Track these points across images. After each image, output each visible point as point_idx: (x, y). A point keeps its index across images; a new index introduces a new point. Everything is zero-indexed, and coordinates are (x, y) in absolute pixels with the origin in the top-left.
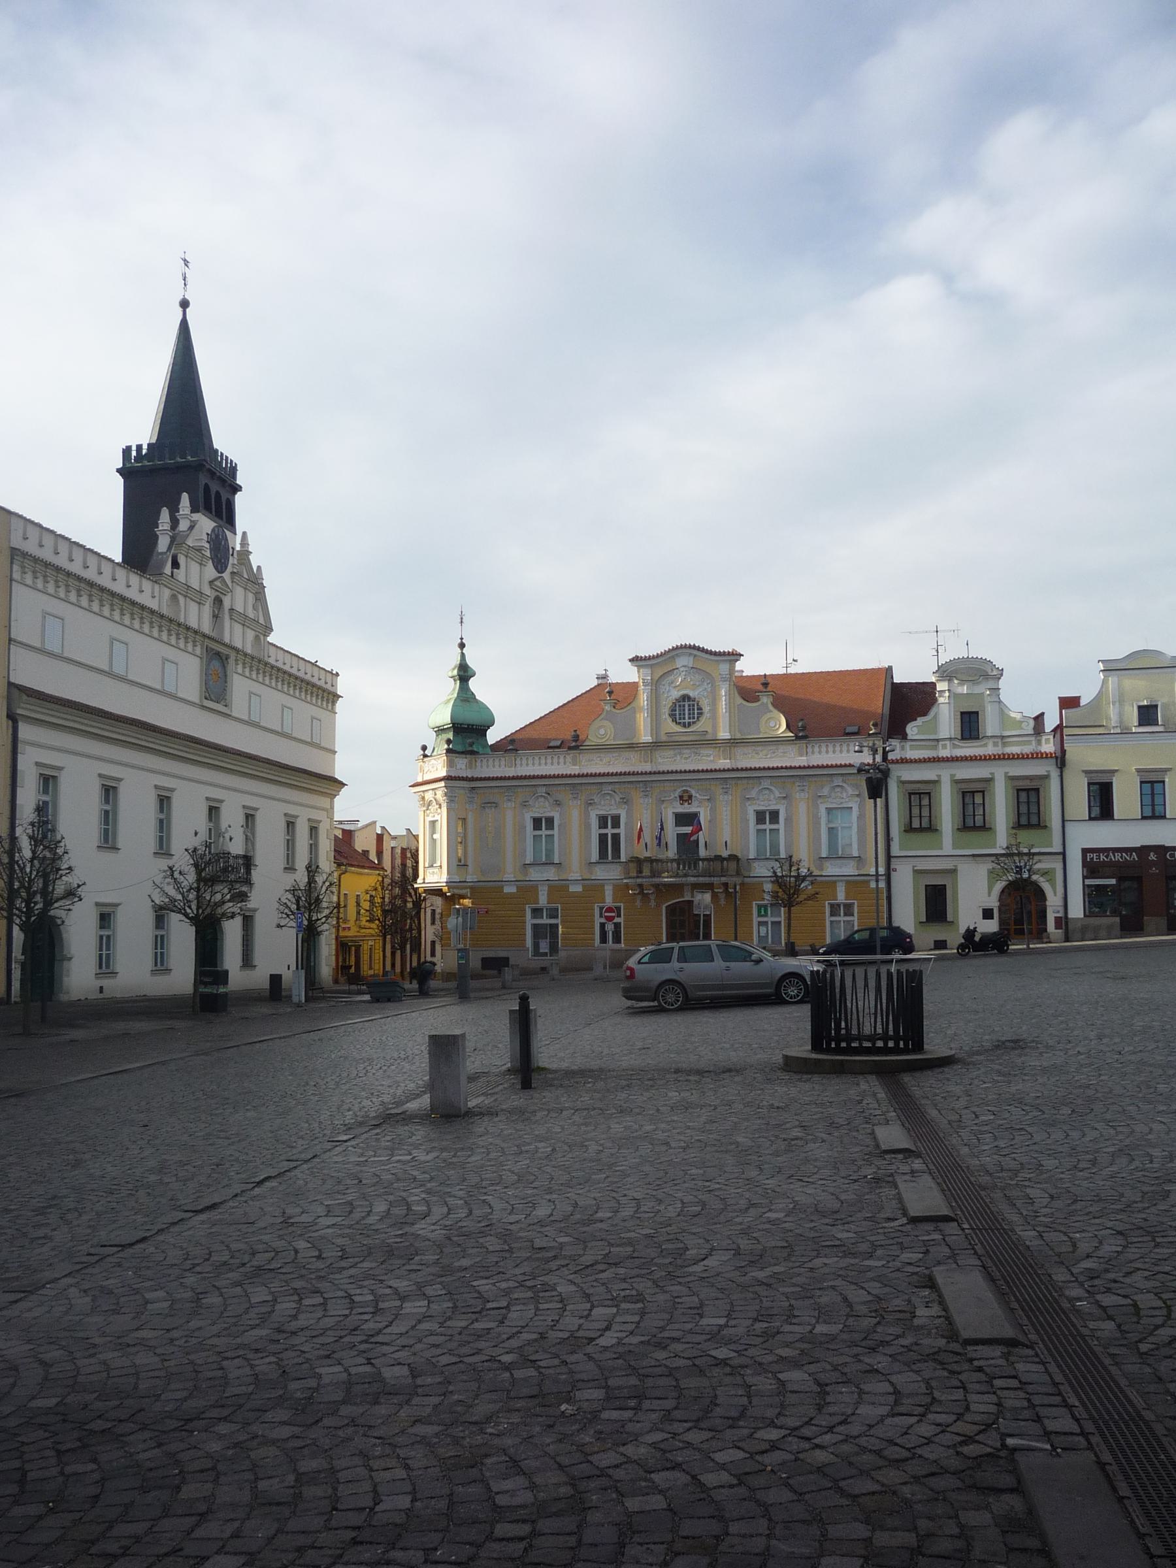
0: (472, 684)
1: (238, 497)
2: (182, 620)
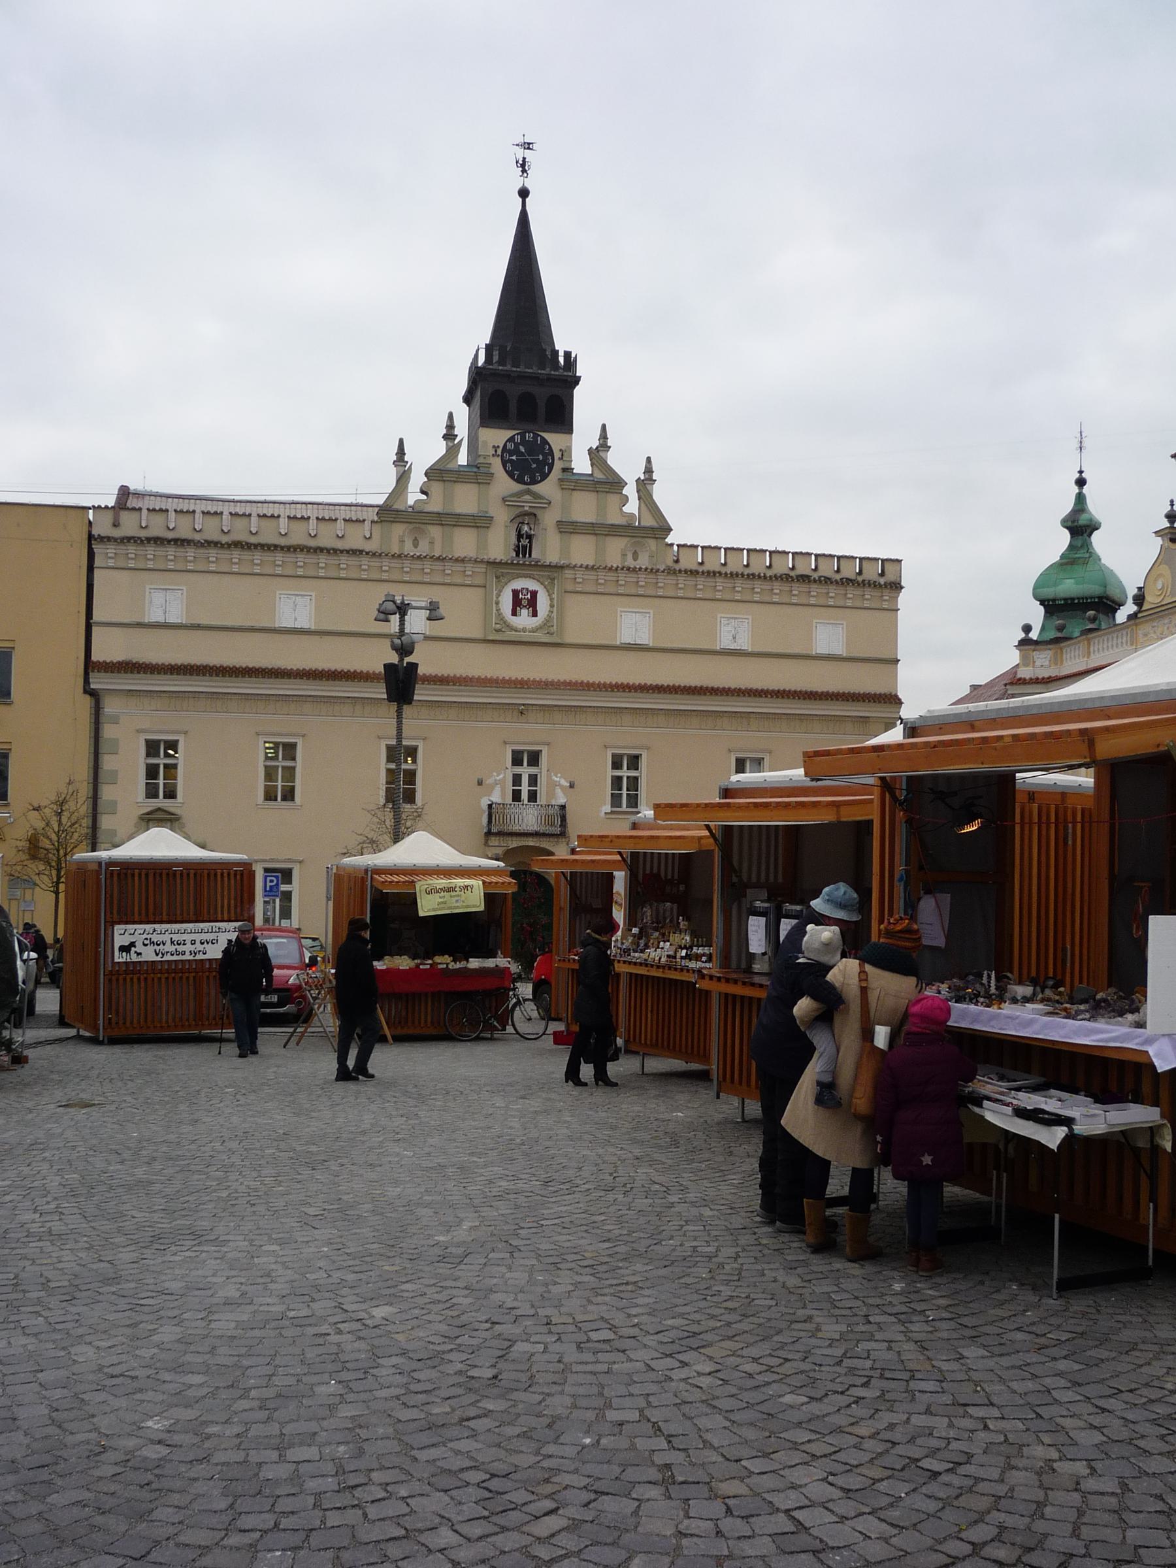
0: (1096, 538)
1: (577, 391)
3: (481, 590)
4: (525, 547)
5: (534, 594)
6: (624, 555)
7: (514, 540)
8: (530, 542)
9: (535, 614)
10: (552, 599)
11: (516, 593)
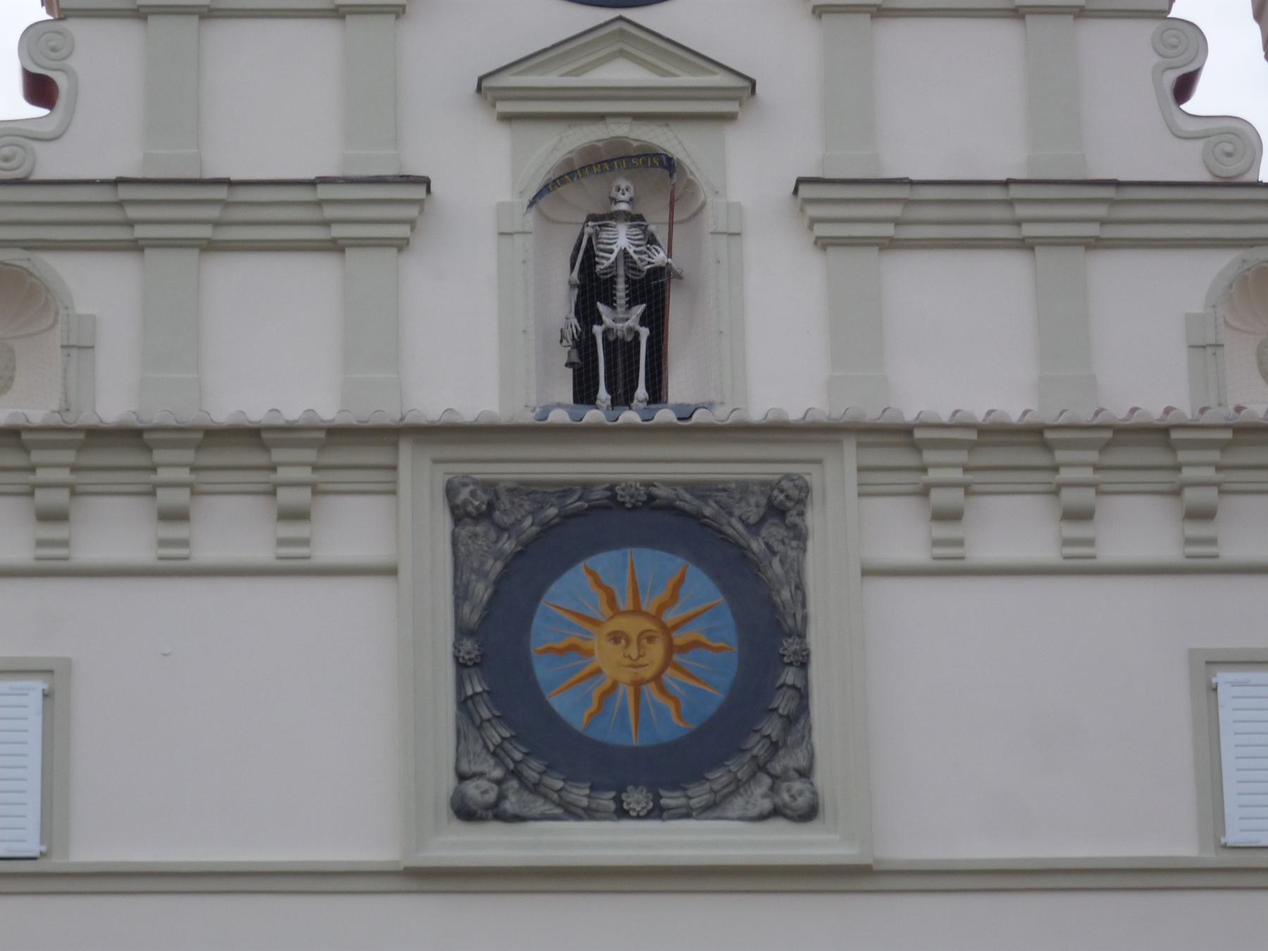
2: (112, 406)
4: (621, 350)
6: (1204, 349)
8: (656, 319)
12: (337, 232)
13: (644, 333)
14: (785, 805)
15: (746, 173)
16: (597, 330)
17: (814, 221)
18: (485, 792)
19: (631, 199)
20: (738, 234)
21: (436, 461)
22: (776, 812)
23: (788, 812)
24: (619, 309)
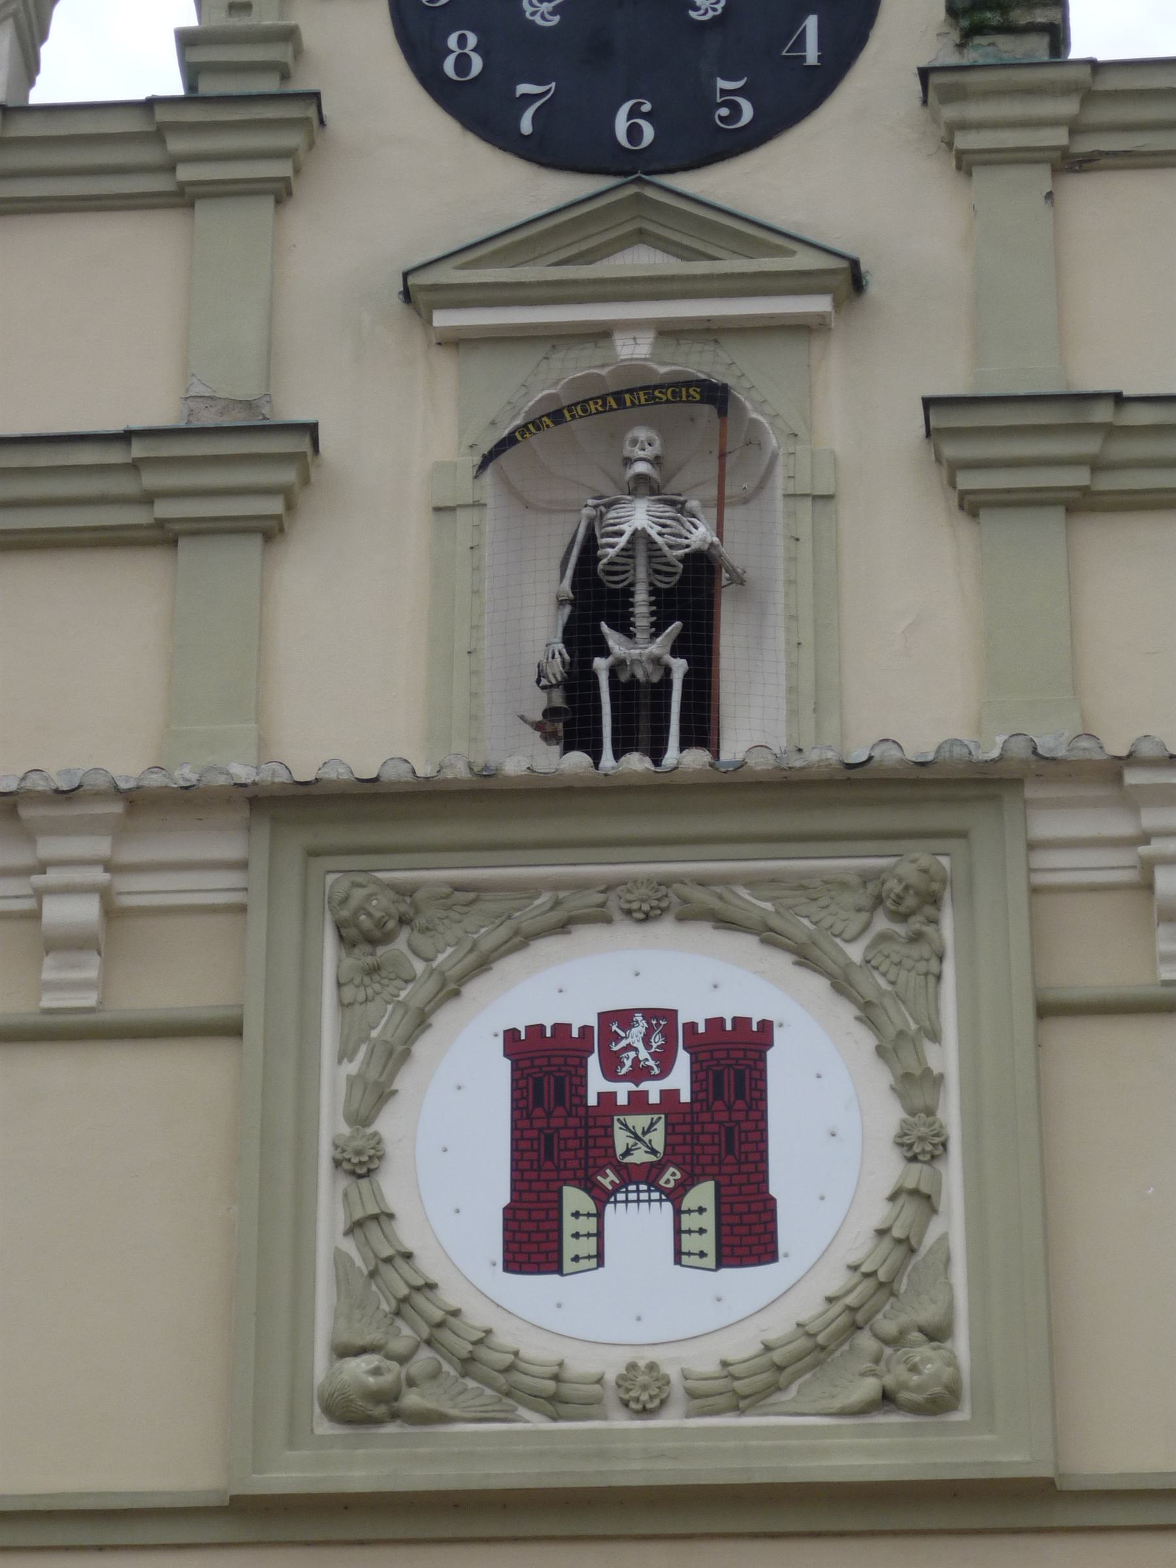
3: (201, 1069)
5: (734, 1060)
7: (541, 630)
8: (699, 646)
9: (747, 1234)
10: (915, 1086)
11: (544, 1067)
12: (165, 510)
13: (679, 667)
14: (904, 1386)
15: (850, 421)
16: (601, 665)
17: (955, 468)
18: (376, 1372)
19: (657, 458)
20: (830, 497)
21: (313, 853)
22: (887, 1399)
23: (904, 1396)
24: (641, 636)
